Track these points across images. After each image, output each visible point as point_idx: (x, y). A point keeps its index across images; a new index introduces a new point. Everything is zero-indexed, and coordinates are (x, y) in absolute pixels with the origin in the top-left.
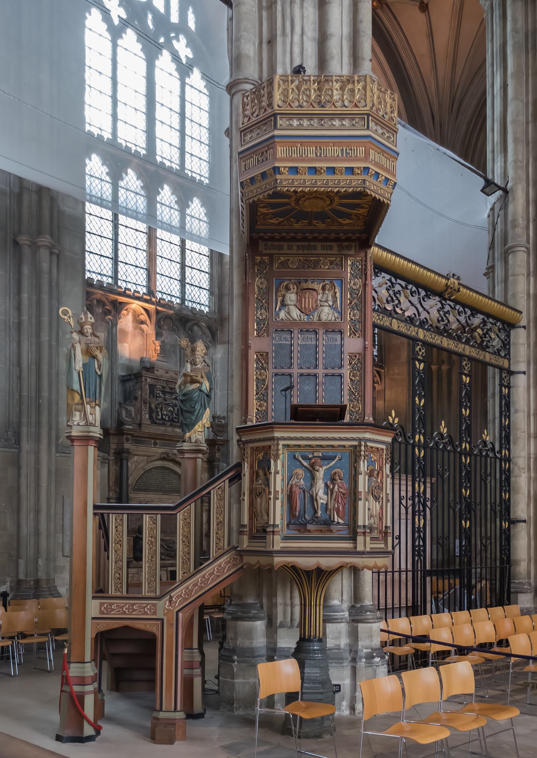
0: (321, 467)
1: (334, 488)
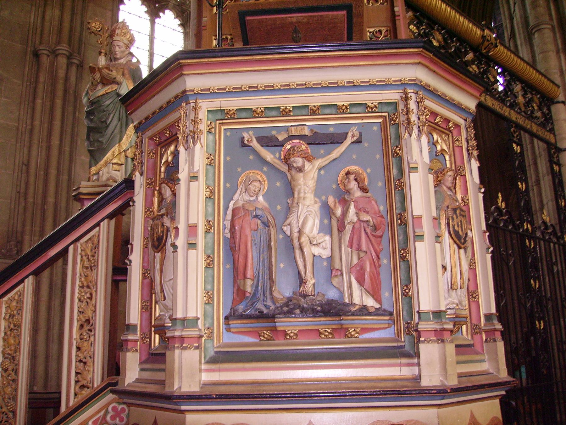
0: (309, 160)
1: (345, 213)
